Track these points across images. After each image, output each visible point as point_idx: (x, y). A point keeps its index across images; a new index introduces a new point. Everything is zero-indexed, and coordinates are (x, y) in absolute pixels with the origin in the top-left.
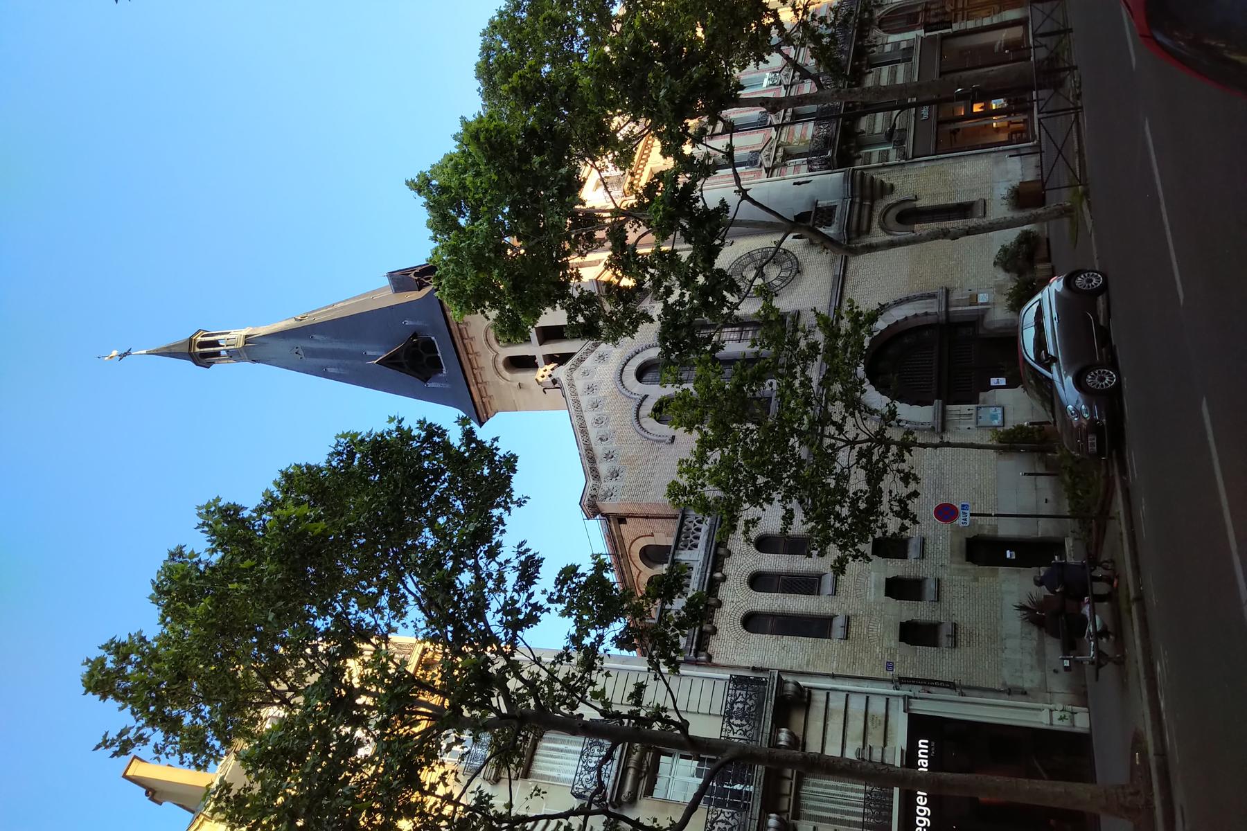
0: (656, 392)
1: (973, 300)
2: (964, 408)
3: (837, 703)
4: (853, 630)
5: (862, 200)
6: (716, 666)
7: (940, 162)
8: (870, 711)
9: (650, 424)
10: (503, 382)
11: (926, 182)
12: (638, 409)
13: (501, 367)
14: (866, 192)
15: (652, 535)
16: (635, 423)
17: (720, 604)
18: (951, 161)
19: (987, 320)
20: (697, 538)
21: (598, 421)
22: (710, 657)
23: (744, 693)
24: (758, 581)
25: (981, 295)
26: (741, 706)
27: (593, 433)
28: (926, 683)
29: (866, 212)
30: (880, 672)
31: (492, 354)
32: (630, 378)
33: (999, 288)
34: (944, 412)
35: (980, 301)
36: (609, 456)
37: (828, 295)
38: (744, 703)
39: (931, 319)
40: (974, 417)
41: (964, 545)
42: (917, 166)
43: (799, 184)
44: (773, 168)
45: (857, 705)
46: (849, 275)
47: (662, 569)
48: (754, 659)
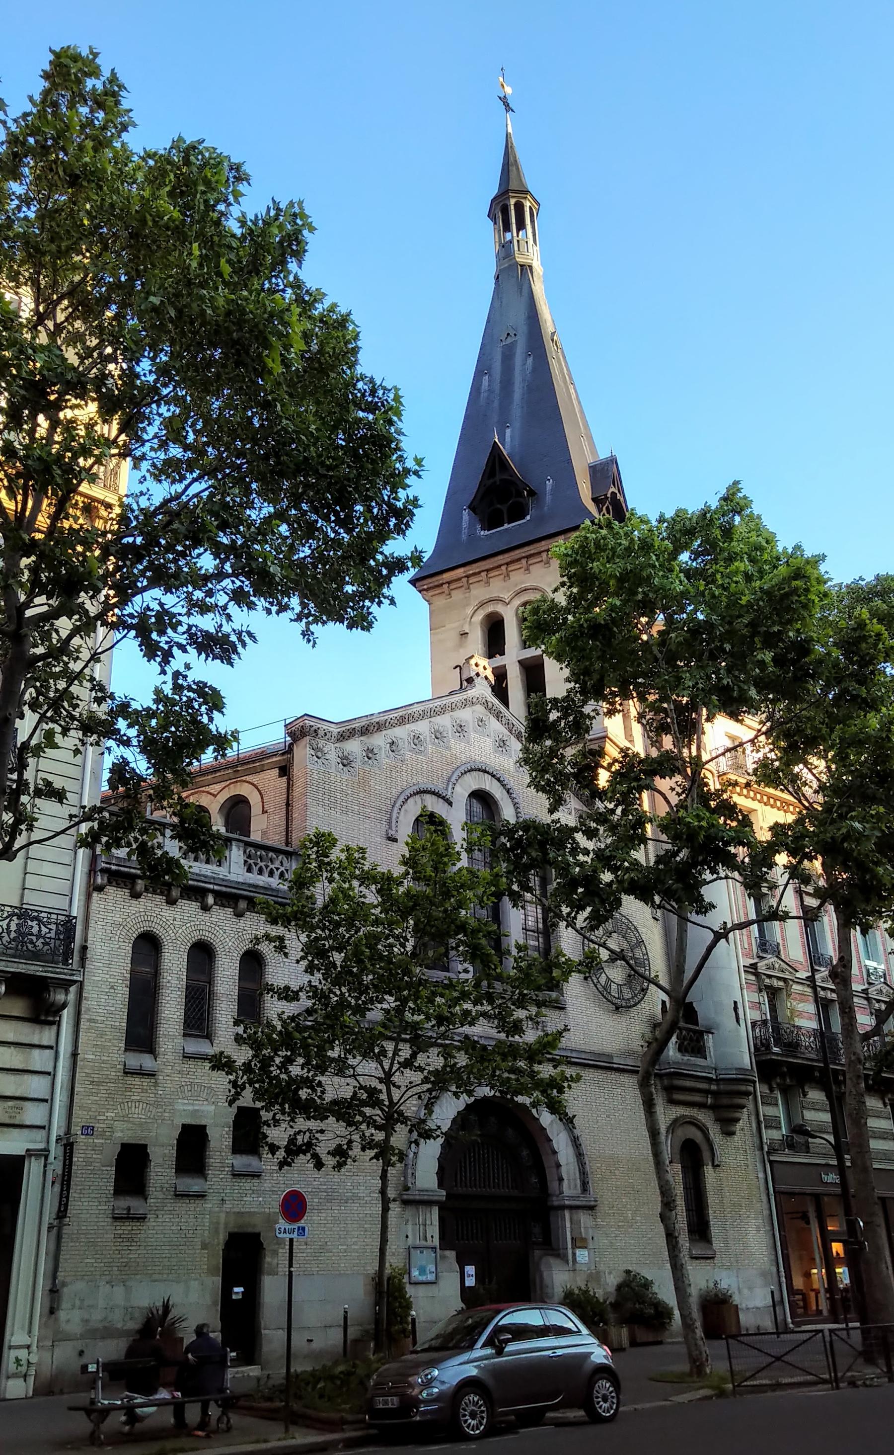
0: (456, 817)
1: (579, 1242)
2: (434, 1231)
3: (39, 1060)
4: (137, 1081)
5: (715, 1094)
6: (89, 897)
7: (764, 1198)
8: (28, 1104)
9: (413, 809)
10: (469, 611)
11: (738, 1178)
12: (433, 793)
13: (490, 609)
14: (724, 1099)
15: (264, 812)
16: (414, 789)
17: (171, 902)
18: (766, 1212)
19: (552, 1261)
20: (261, 872)
21: (417, 739)
22: (100, 889)
23: (52, 935)
24: (202, 954)
25: (585, 1252)
26: (35, 930)
27: (401, 733)
28: (66, 1180)
29: (697, 1098)
30: (80, 1117)
31: (506, 596)
32: (474, 782)
33: (595, 1277)
34: (429, 1203)
35: (578, 1252)
36: (370, 753)
37: (583, 1047)
38: (39, 936)
39: (553, 1185)
40: (423, 1243)
41: (250, 1230)
42: (759, 1166)
43: (736, 1009)
44: (757, 974)
45: (36, 1086)
46: (614, 1075)
47: (218, 825)
48: (98, 948)
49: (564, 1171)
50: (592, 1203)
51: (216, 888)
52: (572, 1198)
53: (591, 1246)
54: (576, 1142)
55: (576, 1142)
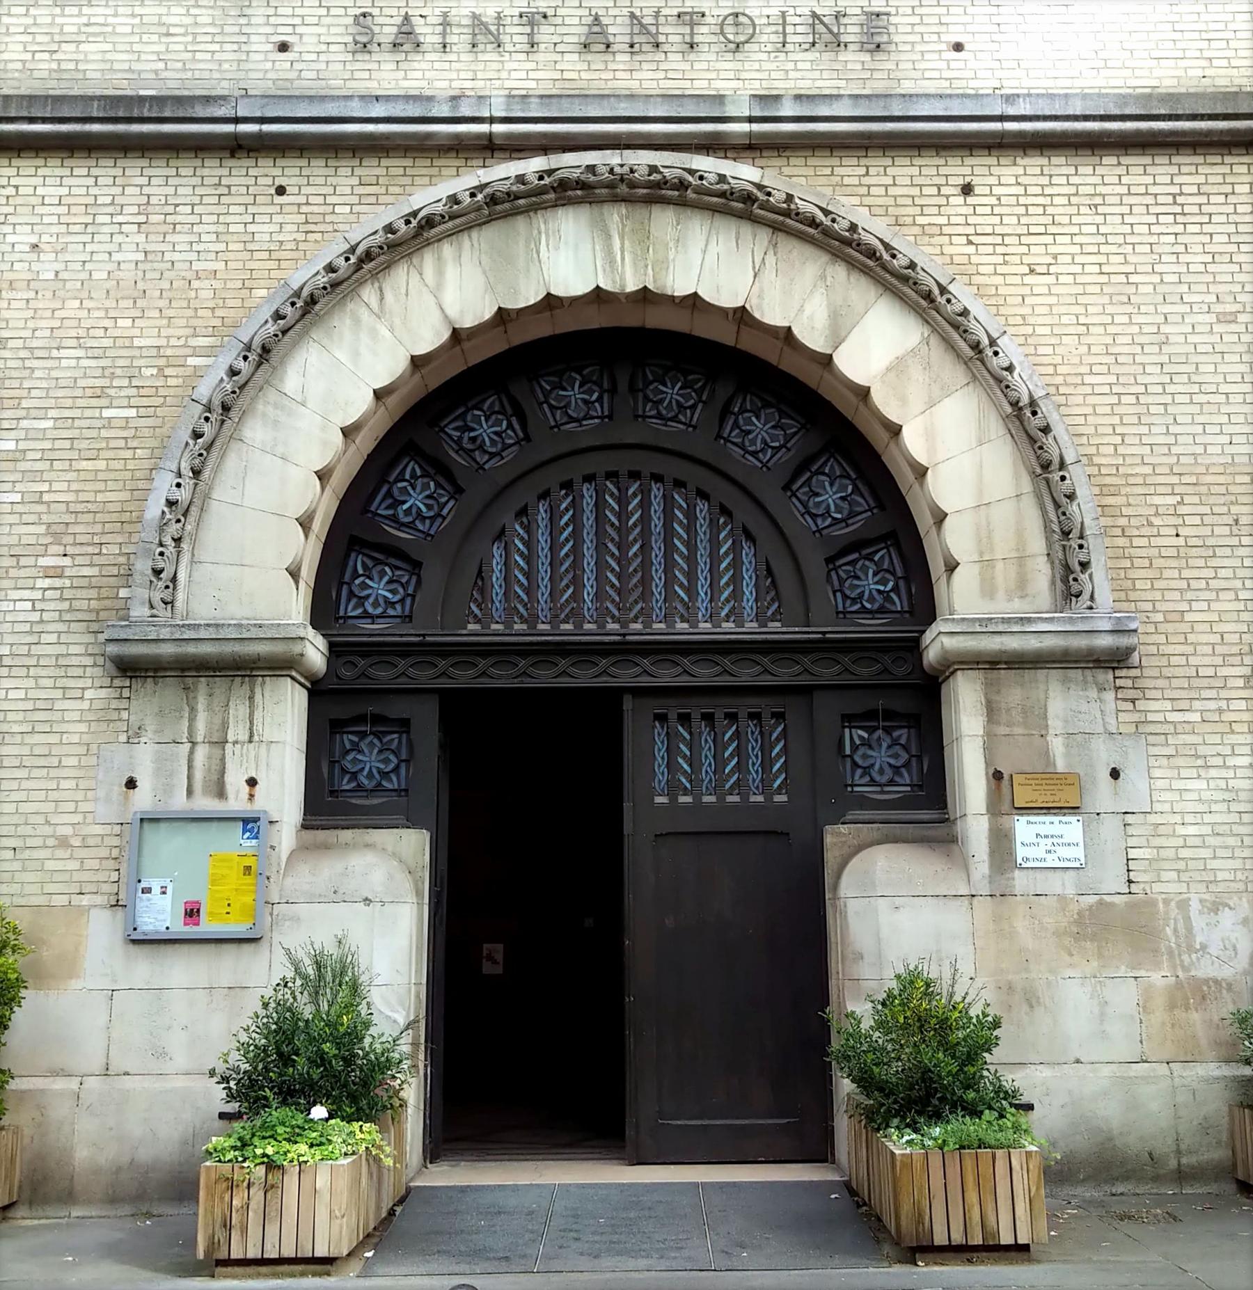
25: (1071, 828)
34: (239, 667)
35: (1024, 829)
40: (206, 804)
49: (957, 538)
50: (1105, 641)
52: (985, 625)
53: (1103, 795)
54: (1025, 423)
55: (1025, 423)
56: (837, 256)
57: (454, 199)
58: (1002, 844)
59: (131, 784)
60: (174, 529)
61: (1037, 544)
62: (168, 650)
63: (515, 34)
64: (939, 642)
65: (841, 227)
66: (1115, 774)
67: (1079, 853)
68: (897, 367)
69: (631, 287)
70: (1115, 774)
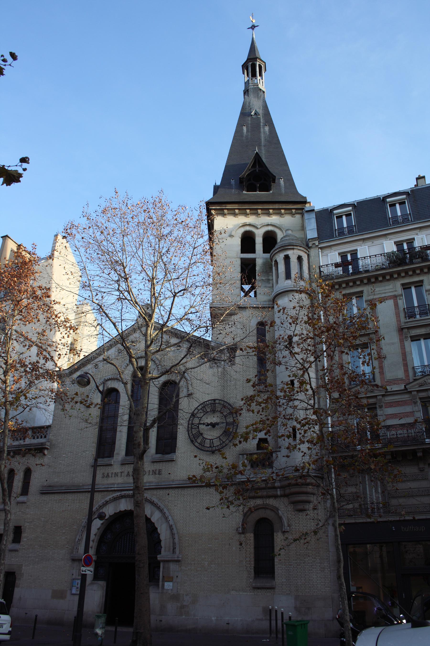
1: (170, 579)
25: (171, 584)
35: (166, 584)
41: (12, 571)
50: (176, 559)
51: (12, 449)
56: (152, 505)
57: (110, 499)
58: (163, 585)
59: (73, 575)
60: (79, 543)
61: (172, 545)
62: (77, 558)
63: (119, 474)
64: (159, 557)
65: (152, 501)
66: (177, 577)
67: (172, 587)
68: (158, 520)
69: (129, 509)
70: (177, 577)
